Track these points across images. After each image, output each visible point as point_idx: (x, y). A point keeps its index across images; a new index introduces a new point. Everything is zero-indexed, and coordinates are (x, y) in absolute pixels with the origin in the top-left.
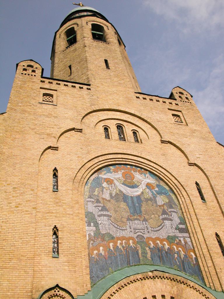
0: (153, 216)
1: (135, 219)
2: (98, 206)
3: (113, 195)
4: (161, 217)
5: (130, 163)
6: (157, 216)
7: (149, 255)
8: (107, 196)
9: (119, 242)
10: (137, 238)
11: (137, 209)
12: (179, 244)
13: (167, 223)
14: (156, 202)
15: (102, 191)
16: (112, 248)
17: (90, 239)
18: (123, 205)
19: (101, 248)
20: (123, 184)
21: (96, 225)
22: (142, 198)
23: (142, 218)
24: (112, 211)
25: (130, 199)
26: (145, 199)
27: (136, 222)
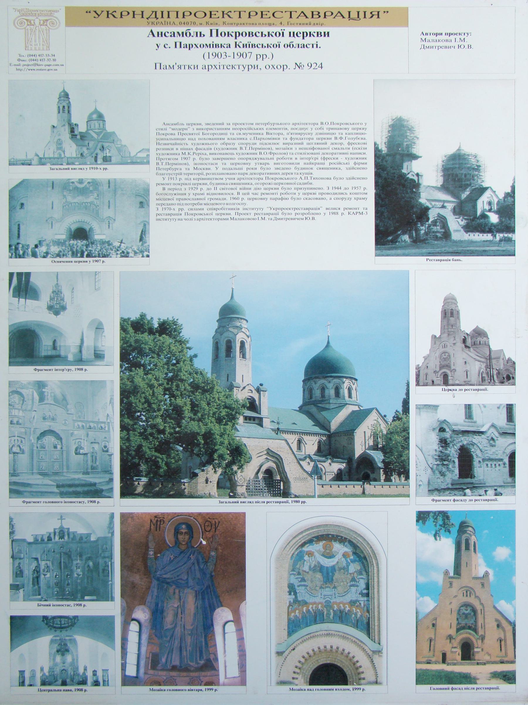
0: (342, 583)
1: (326, 587)
2: (299, 578)
3: (312, 567)
4: (349, 584)
5: (332, 533)
6: (345, 583)
7: (331, 616)
8: (306, 568)
9: (311, 606)
10: (325, 602)
11: (330, 578)
12: (359, 606)
13: (353, 589)
14: (348, 571)
15: (304, 564)
16: (305, 611)
17: (290, 605)
18: (319, 576)
19: (297, 611)
20: (323, 555)
21: (295, 594)
22: (336, 568)
23: (332, 587)
24: (309, 582)
25: (325, 569)
26: (338, 567)
27: (327, 589)
